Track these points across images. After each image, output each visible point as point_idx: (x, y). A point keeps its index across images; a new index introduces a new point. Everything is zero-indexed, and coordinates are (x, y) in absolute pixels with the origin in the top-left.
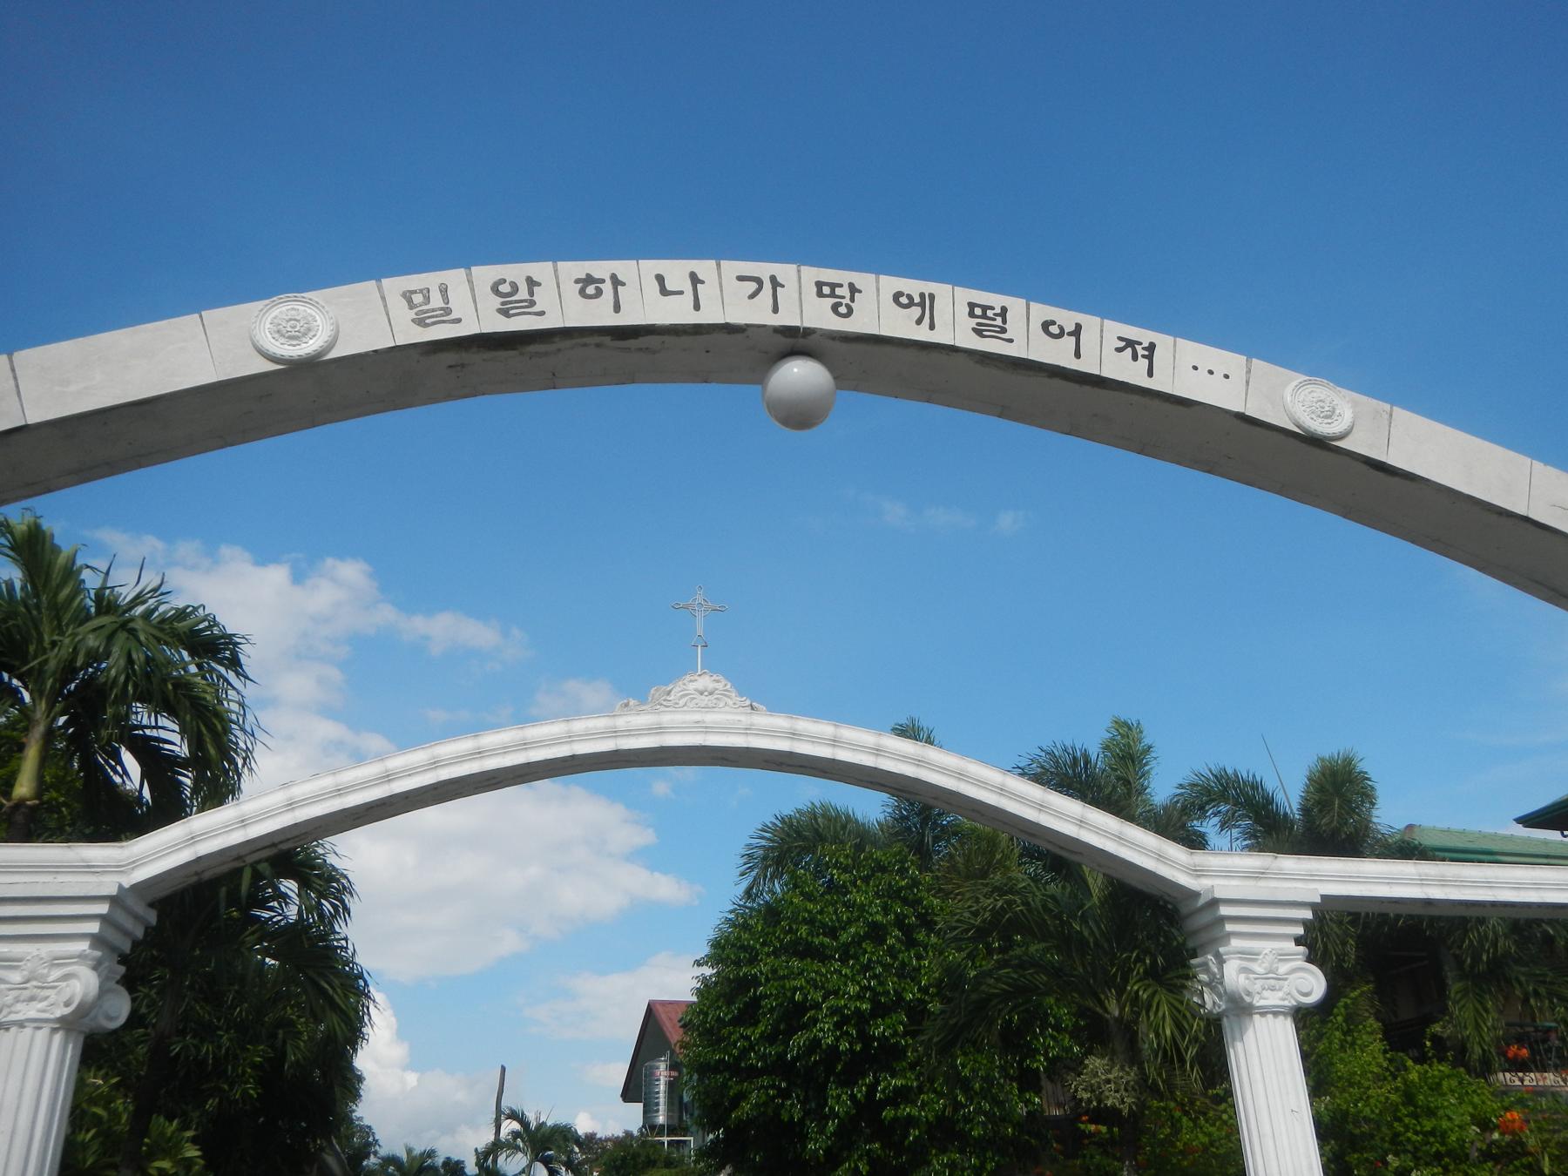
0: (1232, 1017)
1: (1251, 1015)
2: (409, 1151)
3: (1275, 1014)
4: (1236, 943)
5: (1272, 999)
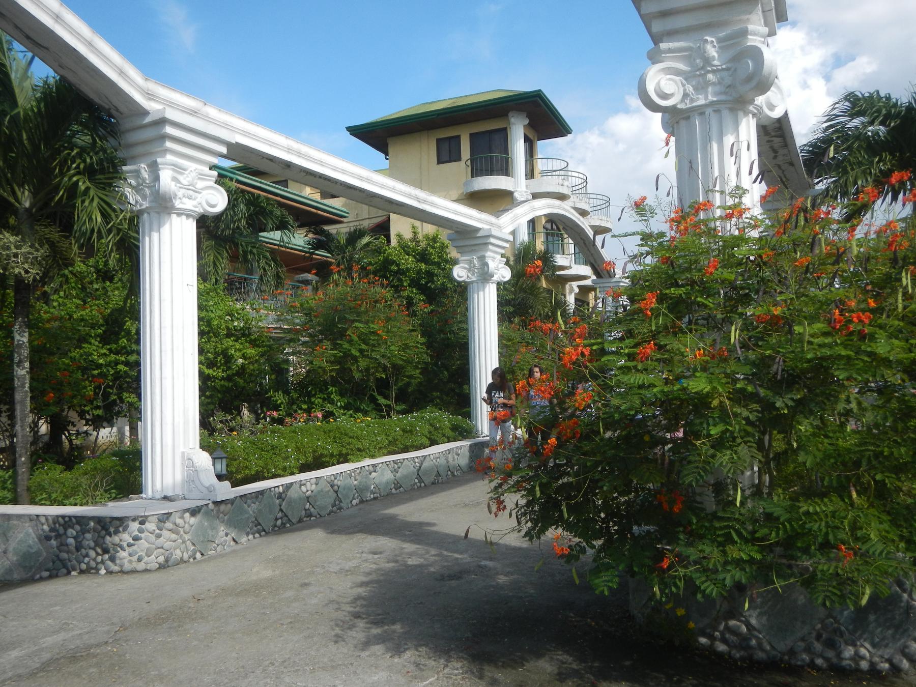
0: (153, 214)
1: (169, 214)
3: (188, 216)
4: (169, 157)
5: (188, 205)
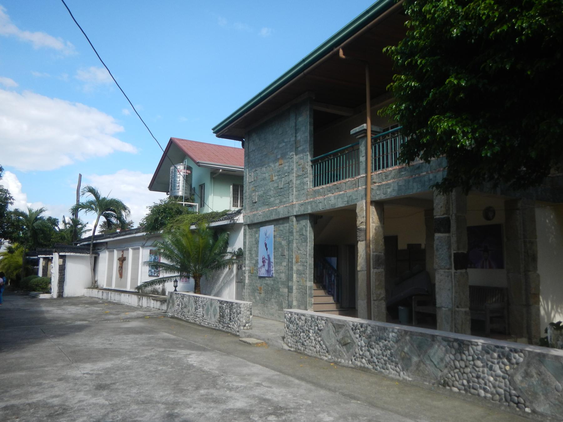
2: (30, 211)
